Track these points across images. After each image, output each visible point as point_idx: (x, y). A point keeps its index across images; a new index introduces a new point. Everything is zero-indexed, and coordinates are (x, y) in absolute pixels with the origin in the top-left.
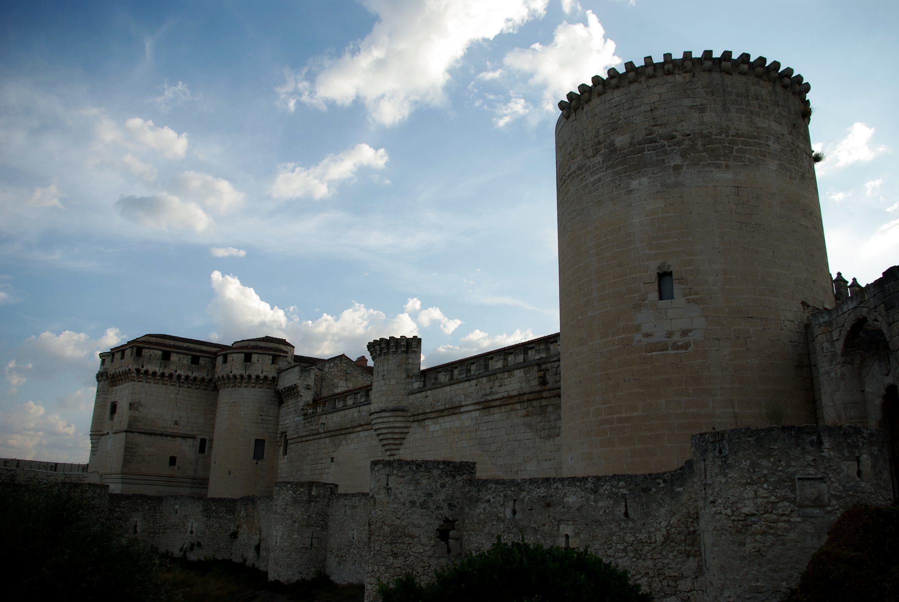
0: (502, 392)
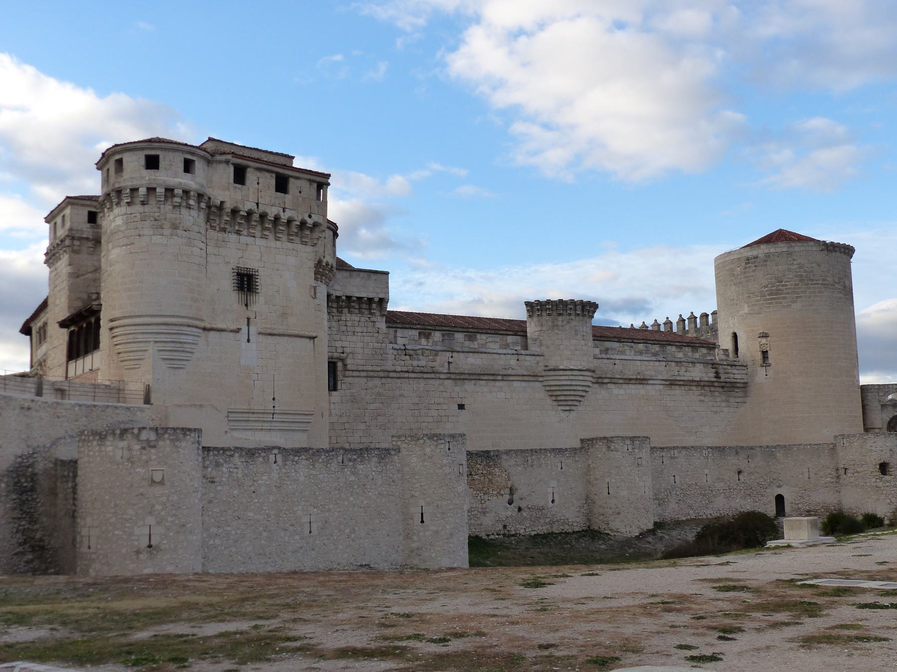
0: (687, 376)
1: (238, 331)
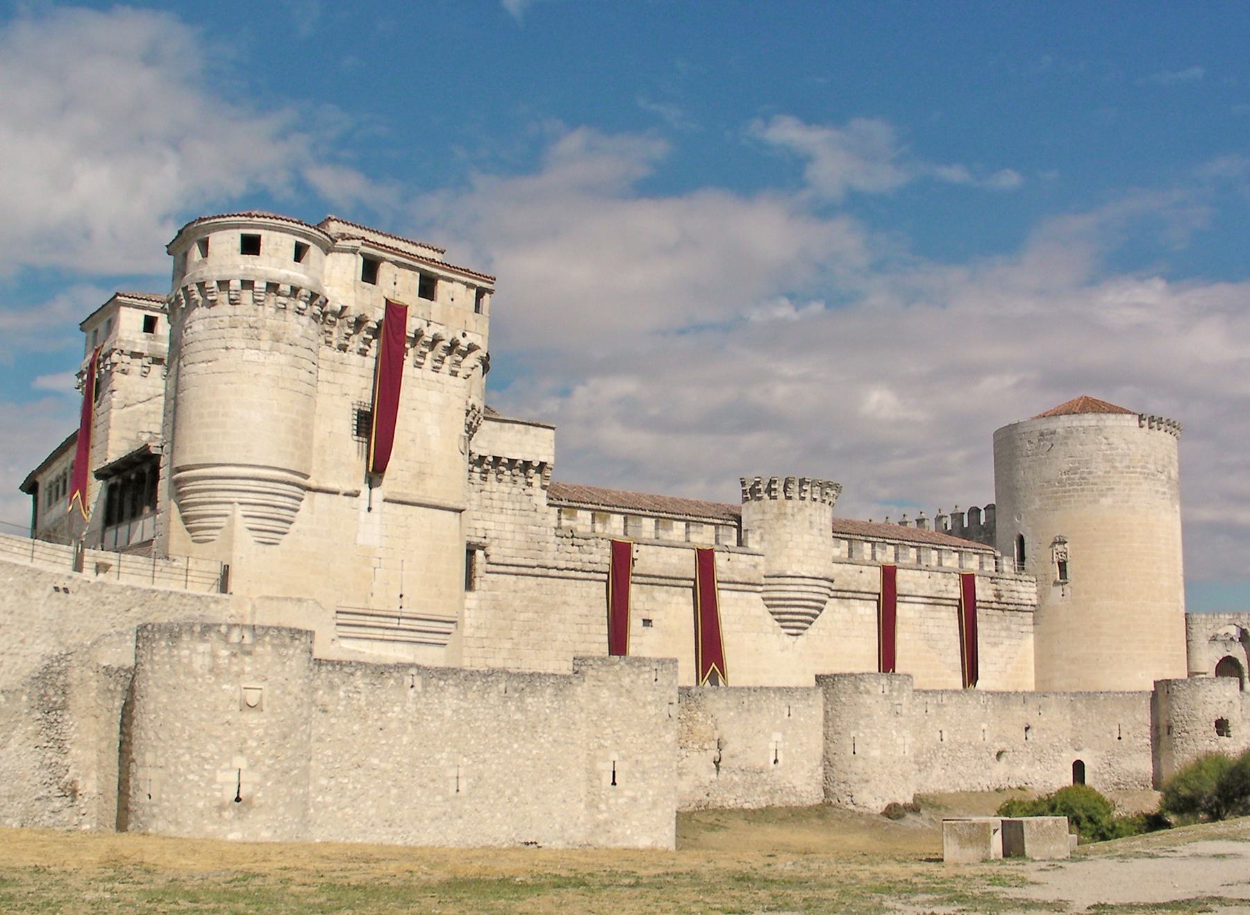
1: (356, 494)
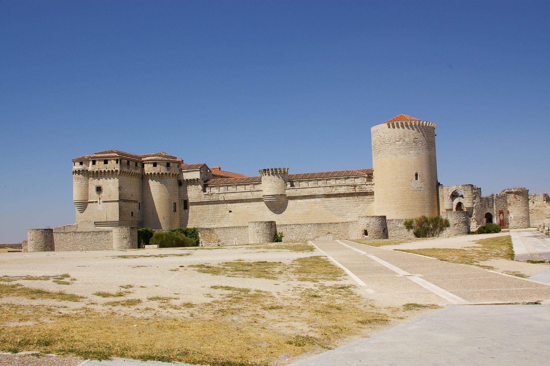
0: (336, 192)
1: (96, 202)
